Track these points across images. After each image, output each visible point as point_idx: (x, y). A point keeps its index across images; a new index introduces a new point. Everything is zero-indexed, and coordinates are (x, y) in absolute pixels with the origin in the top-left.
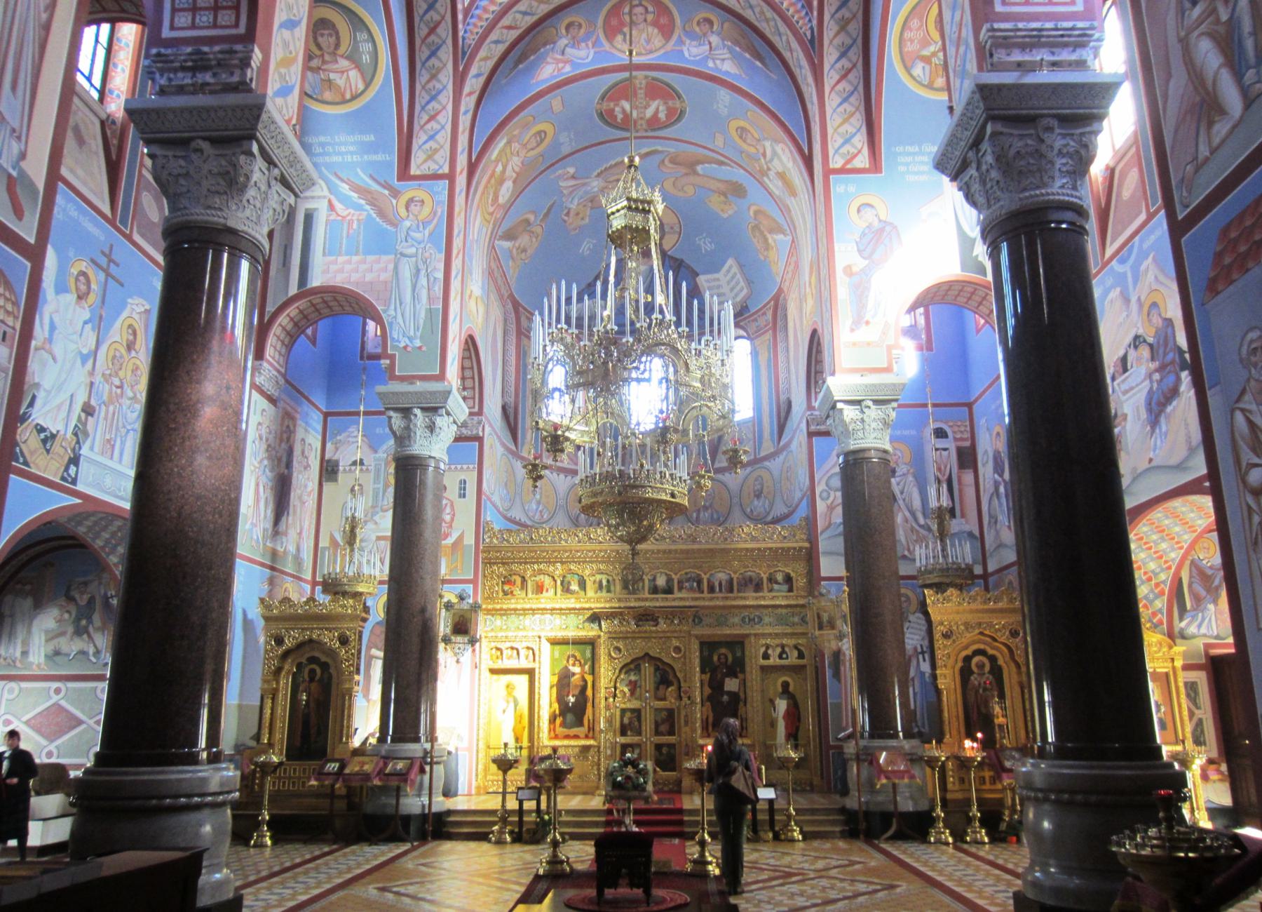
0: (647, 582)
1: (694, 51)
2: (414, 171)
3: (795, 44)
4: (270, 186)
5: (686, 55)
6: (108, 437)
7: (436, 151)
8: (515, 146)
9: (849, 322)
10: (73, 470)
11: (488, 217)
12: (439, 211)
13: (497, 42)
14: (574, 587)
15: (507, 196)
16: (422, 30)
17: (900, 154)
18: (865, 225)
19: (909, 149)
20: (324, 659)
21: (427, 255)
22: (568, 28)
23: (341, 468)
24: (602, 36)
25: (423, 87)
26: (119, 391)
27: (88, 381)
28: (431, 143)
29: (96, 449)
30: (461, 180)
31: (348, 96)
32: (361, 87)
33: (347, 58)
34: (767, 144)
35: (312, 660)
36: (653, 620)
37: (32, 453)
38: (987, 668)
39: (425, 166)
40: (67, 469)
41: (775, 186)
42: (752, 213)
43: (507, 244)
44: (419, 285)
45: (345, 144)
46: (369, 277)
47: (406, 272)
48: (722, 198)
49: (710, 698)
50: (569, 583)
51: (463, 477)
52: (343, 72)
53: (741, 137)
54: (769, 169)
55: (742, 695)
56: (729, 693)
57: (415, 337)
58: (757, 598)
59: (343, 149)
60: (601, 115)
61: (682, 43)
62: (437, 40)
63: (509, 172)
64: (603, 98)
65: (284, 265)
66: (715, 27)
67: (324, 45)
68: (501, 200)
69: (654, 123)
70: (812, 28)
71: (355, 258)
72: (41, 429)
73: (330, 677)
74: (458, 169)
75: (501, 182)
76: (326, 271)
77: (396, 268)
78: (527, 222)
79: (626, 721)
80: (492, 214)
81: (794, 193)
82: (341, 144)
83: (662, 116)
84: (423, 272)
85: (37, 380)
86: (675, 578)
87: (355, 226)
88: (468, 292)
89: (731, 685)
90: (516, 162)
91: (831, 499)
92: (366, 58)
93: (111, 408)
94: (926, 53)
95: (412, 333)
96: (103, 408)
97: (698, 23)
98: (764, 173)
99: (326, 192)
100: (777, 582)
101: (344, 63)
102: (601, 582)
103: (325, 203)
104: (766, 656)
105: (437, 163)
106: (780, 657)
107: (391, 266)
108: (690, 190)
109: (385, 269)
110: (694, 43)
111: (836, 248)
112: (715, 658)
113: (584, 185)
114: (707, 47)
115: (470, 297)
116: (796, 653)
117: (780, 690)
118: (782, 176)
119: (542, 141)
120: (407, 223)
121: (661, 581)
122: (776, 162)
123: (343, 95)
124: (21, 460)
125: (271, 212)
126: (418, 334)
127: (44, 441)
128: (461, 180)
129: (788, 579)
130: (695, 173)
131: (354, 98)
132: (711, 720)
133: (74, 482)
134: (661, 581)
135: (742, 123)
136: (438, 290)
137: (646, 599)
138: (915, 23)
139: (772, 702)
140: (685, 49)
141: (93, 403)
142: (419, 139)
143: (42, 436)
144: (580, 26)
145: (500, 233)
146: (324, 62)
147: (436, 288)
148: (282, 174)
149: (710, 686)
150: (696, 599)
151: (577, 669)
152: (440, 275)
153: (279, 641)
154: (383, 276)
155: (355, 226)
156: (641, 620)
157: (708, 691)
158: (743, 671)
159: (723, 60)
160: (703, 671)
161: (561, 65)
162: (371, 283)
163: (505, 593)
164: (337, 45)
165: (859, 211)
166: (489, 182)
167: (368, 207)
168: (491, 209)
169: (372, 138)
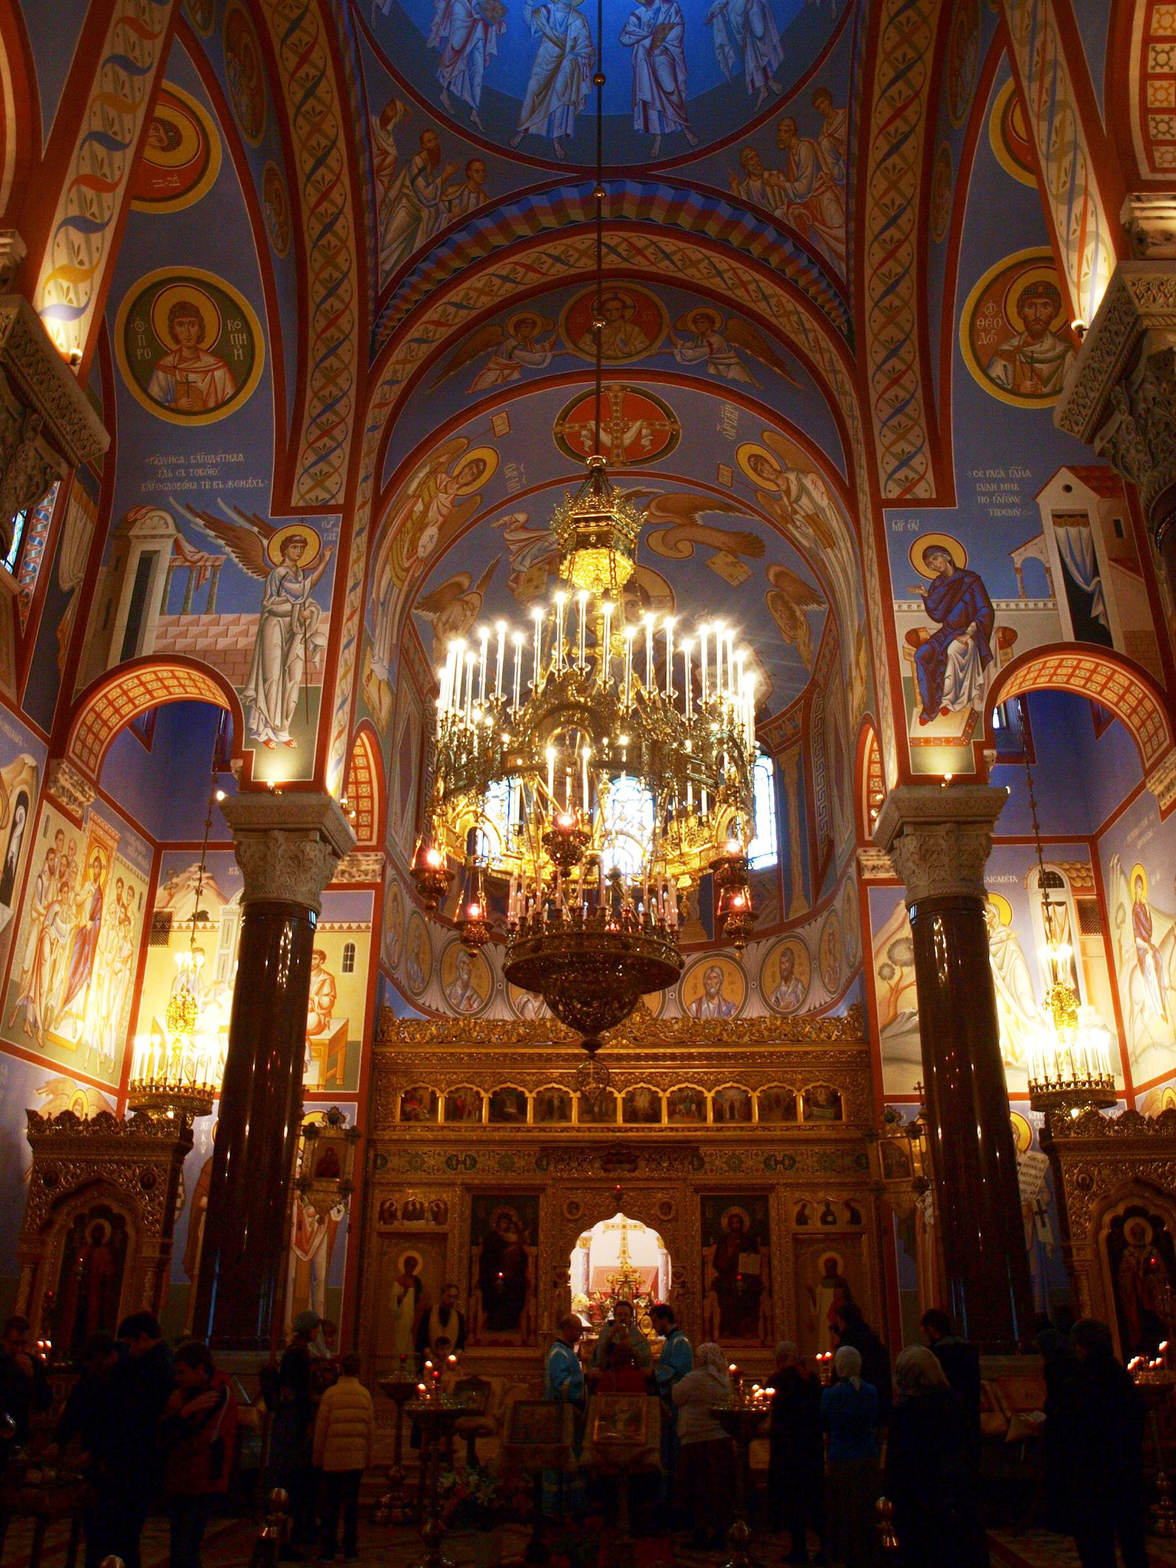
1: (690, 353)
2: (295, 501)
3: (826, 343)
4: (22, 440)
5: (678, 358)
7: (328, 475)
8: (442, 477)
9: (918, 711)
11: (402, 574)
12: (328, 554)
13: (420, 341)
15: (430, 547)
16: (317, 323)
17: (979, 480)
18: (933, 575)
19: (990, 473)
20: (116, 1209)
21: (307, 613)
22: (517, 326)
23: (175, 925)
24: (564, 338)
25: (316, 394)
28: (322, 466)
30: (362, 517)
31: (212, 404)
32: (230, 391)
33: (212, 354)
34: (792, 476)
35: (104, 1211)
38: (1149, 1237)
39: (312, 495)
41: (804, 535)
42: (771, 577)
43: (430, 616)
44: (291, 658)
45: (203, 466)
46: (222, 643)
47: (275, 636)
48: (731, 559)
49: (716, 1286)
51: (351, 941)
52: (207, 372)
53: (755, 470)
54: (795, 512)
55: (764, 1278)
56: (748, 1277)
57: (282, 729)
58: (788, 1129)
59: (200, 472)
60: (561, 440)
61: (670, 343)
62: (337, 334)
63: (432, 514)
64: (563, 417)
65: (105, 627)
66: (717, 325)
67: (182, 337)
68: (421, 552)
69: (634, 453)
70: (848, 321)
71: (205, 618)
73: (125, 1236)
74: (359, 500)
75: (421, 527)
76: (162, 636)
77: (261, 634)
78: (459, 585)
80: (407, 570)
81: (832, 544)
82: (199, 466)
83: (645, 442)
84: (299, 637)
86: (664, 1096)
87: (208, 574)
88: (366, 672)
89: (748, 1263)
90: (444, 500)
91: (896, 977)
92: (239, 353)
94: (1006, 347)
95: (278, 722)
97: (694, 321)
98: (789, 518)
99: (172, 530)
100: (818, 1105)
101: (208, 360)
102: (550, 1101)
103: (171, 542)
104: (802, 1219)
105: (329, 492)
106: (824, 1221)
107: (254, 629)
108: (686, 548)
109: (246, 633)
110: (689, 344)
111: (896, 607)
112: (724, 1222)
113: (539, 538)
114: (707, 350)
115: (369, 677)
116: (847, 1215)
117: (823, 1272)
118: (814, 520)
119: (480, 473)
120: (282, 571)
121: (642, 1102)
122: (804, 500)
123: (205, 402)
125: (22, 478)
126: (287, 723)
128: (362, 517)
129: (834, 1100)
130: (694, 524)
131: (219, 406)
132: (717, 1320)
134: (642, 1102)
135: (757, 450)
136: (319, 660)
137: (619, 1130)
138: (990, 308)
139: (811, 1290)
140: (676, 352)
142: (306, 458)
144: (534, 323)
145: (419, 599)
146: (182, 359)
147: (317, 659)
148: (45, 426)
149: (716, 1265)
150: (696, 1130)
151: (512, 1237)
152: (322, 641)
153: (51, 1180)
154: (243, 642)
155: (208, 574)
156: (610, 1161)
157: (712, 1273)
158: (767, 1242)
159: (728, 365)
160: (705, 1243)
161: (506, 372)
162: (225, 652)
163: (406, 1116)
164: (201, 338)
165: (925, 556)
166: (403, 524)
167: (228, 549)
168: (407, 565)
169: (241, 458)
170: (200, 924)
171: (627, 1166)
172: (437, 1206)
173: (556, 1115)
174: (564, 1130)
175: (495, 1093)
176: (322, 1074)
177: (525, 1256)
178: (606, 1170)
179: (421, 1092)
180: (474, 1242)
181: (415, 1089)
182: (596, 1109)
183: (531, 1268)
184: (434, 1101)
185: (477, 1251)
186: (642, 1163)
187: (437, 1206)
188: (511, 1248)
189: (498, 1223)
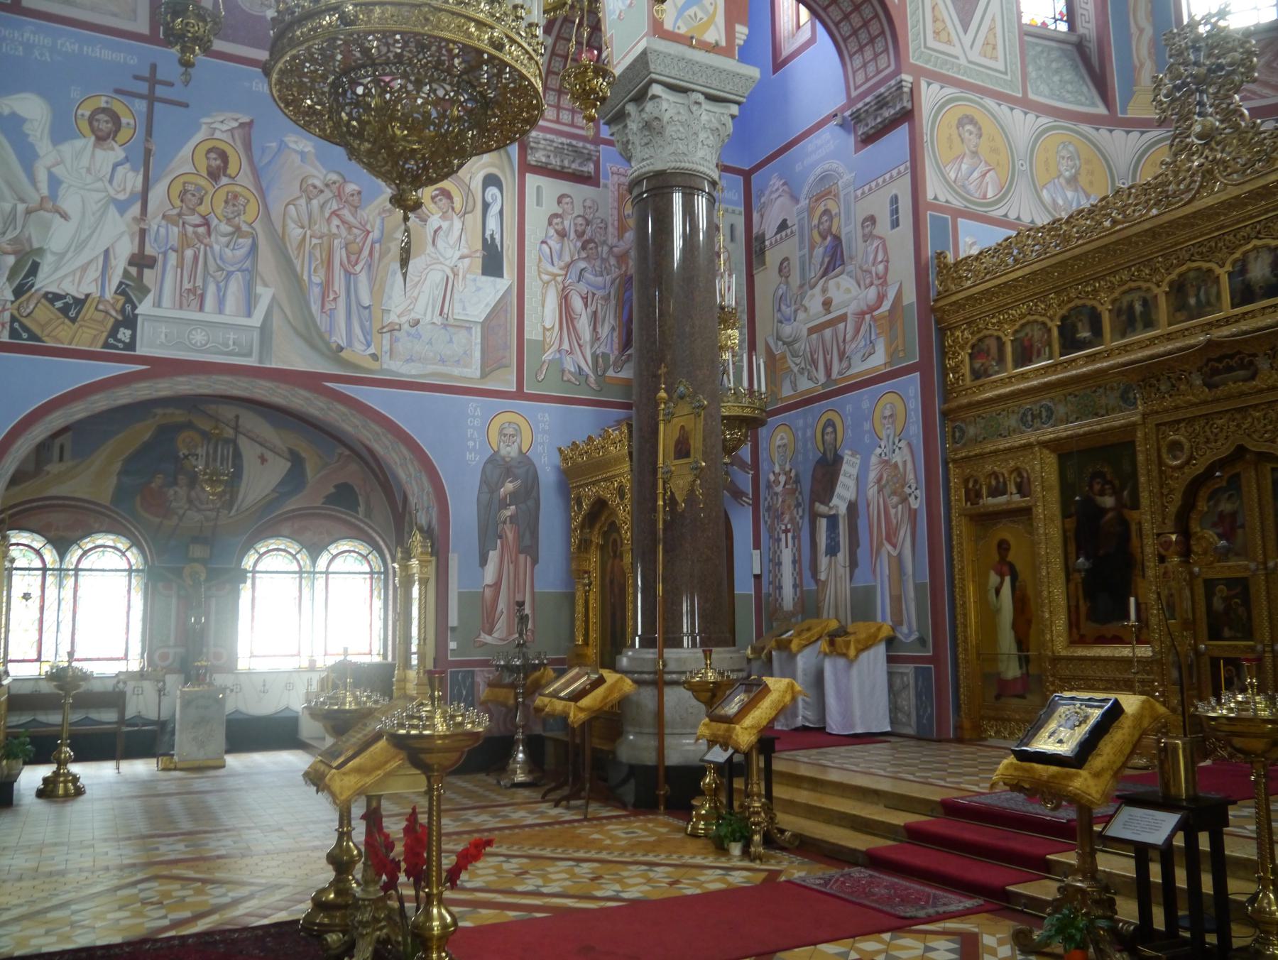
0: (1225, 280)
6: (187, 286)
10: (125, 334)
14: (1085, 334)
26: (201, 230)
27: (136, 228)
29: (166, 301)
36: (1242, 366)
37: (43, 327)
40: (113, 333)
50: (1074, 330)
51: (894, 192)
72: (52, 298)
79: (1218, 604)
85: (36, 245)
93: (189, 253)
96: (173, 257)
102: (1131, 307)
127: (65, 310)
133: (131, 345)
141: (149, 250)
143: (59, 304)
151: (1108, 501)
156: (1216, 372)
163: (976, 375)
170: (784, 234)
171: (1242, 373)
172: (1020, 475)
173: (1139, 325)
174: (1152, 342)
175: (1063, 319)
176: (887, 350)
177: (1125, 523)
178: (1210, 386)
179: (987, 341)
180: (1065, 515)
181: (980, 340)
182: (1192, 301)
183: (1135, 541)
184: (1001, 345)
185: (1071, 523)
186: (1263, 364)
187: (1020, 475)
188: (1110, 515)
189: (1091, 487)
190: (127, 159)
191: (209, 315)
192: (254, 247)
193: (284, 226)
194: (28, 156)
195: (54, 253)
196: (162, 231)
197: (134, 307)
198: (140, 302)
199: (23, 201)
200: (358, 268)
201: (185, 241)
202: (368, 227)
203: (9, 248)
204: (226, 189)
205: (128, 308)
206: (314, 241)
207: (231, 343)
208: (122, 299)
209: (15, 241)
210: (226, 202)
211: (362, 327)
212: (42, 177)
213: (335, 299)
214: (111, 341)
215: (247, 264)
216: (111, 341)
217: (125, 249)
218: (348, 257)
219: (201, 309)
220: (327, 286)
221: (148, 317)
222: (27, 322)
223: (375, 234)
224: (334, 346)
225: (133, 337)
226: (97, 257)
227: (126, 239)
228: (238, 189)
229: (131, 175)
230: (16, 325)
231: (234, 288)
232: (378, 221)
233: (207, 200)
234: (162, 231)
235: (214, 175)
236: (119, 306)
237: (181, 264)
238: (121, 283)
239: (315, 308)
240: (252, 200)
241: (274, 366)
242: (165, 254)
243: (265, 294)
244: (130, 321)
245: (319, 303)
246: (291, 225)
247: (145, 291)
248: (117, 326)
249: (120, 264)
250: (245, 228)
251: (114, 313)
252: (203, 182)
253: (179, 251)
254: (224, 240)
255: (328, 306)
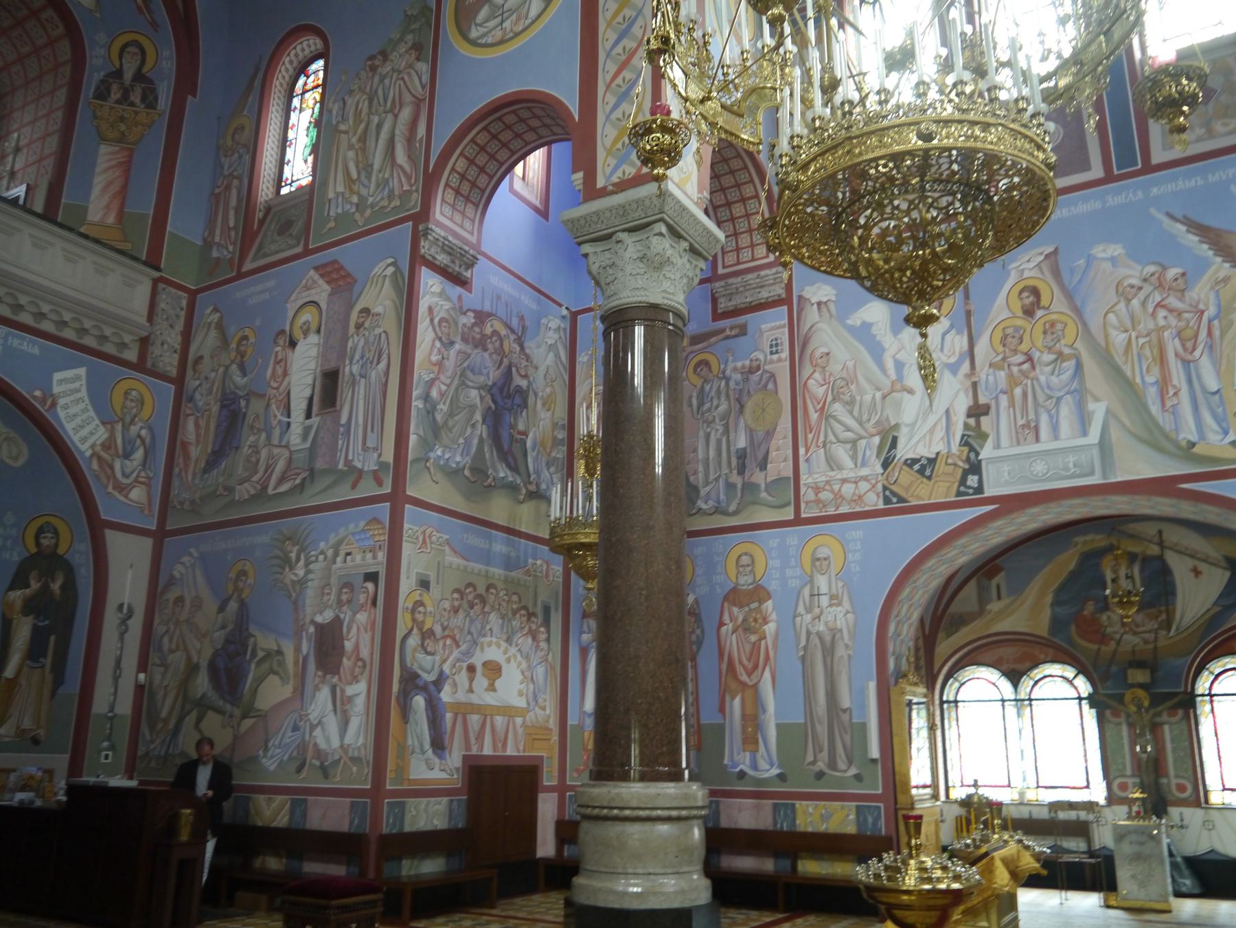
6: (1021, 422)
26: (1026, 366)
27: (968, 383)
29: (1004, 442)
37: (907, 490)
40: (963, 482)
72: (910, 463)
85: (893, 423)
93: (1018, 391)
96: (1004, 400)
124: (895, 500)
127: (921, 472)
133: (979, 489)
141: (982, 400)
143: (917, 467)
190: (952, 326)
191: (1046, 443)
192: (1079, 367)
193: (1106, 336)
194: (877, 351)
195: (907, 425)
196: (991, 378)
197: (977, 454)
198: (982, 447)
199: (878, 389)
200: (1197, 354)
201: (1013, 381)
202: (1201, 307)
203: (874, 431)
204: (1042, 321)
205: (972, 455)
206: (1141, 341)
207: (1071, 465)
208: (966, 449)
209: (878, 423)
210: (1045, 332)
211: (1215, 416)
212: (890, 364)
213: (1175, 394)
214: (962, 489)
215: (1075, 385)
216: (962, 489)
217: (962, 404)
218: (1183, 346)
219: (1037, 440)
220: (1164, 383)
221: (993, 460)
222: (893, 488)
223: (1212, 311)
224: (1184, 443)
225: (980, 481)
226: (940, 419)
227: (962, 395)
228: (1054, 317)
229: (957, 338)
230: (887, 493)
231: (1066, 412)
232: (1212, 296)
233: (1026, 337)
234: (991, 378)
235: (1029, 312)
236: (964, 457)
237: (1012, 404)
238: (963, 436)
239: (1155, 409)
240: (1070, 322)
241: (1119, 479)
242: (996, 398)
243: (1098, 410)
244: (975, 468)
245: (1158, 402)
246: (1113, 333)
247: (983, 437)
248: (966, 473)
249: (960, 418)
250: (1067, 351)
251: (961, 464)
252: (1019, 322)
253: (1009, 392)
254: (1049, 368)
255: (1169, 404)
